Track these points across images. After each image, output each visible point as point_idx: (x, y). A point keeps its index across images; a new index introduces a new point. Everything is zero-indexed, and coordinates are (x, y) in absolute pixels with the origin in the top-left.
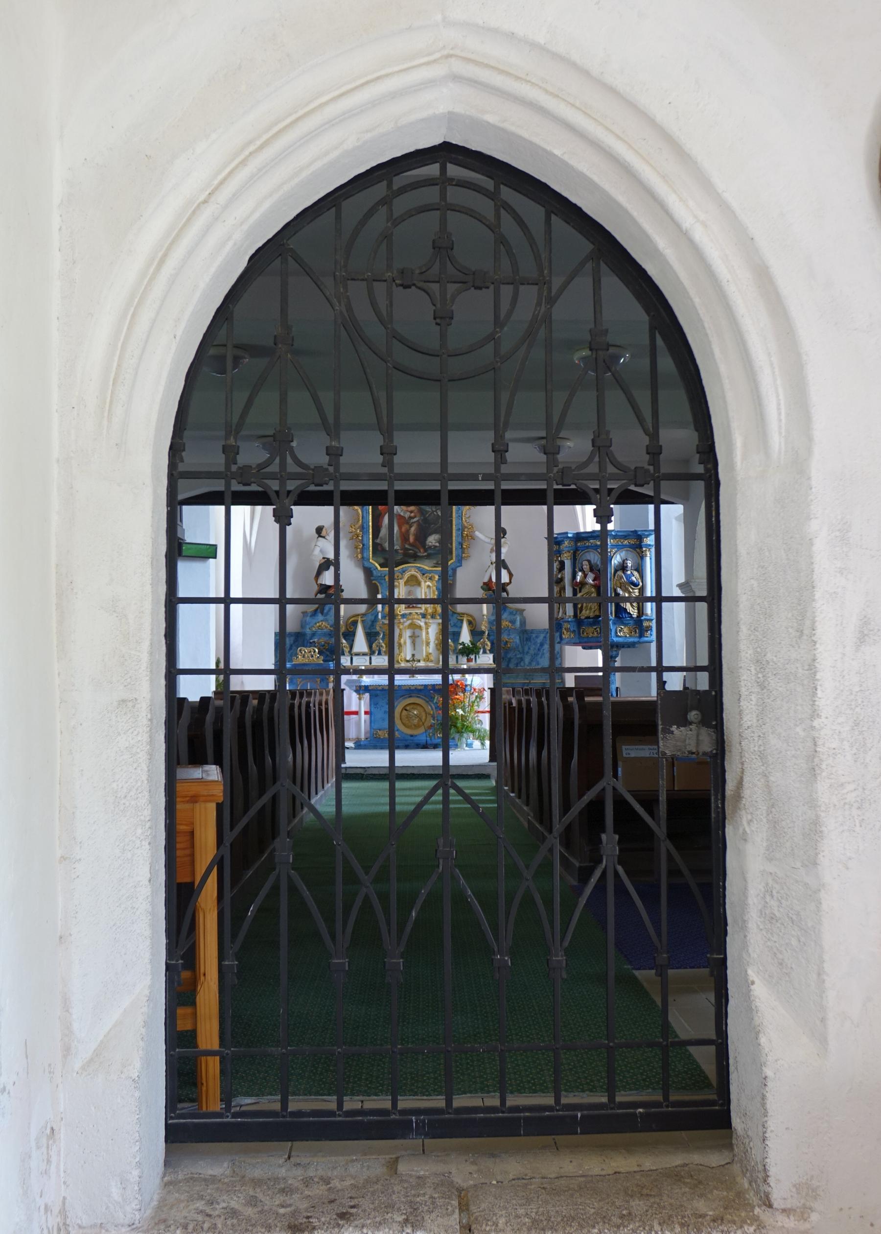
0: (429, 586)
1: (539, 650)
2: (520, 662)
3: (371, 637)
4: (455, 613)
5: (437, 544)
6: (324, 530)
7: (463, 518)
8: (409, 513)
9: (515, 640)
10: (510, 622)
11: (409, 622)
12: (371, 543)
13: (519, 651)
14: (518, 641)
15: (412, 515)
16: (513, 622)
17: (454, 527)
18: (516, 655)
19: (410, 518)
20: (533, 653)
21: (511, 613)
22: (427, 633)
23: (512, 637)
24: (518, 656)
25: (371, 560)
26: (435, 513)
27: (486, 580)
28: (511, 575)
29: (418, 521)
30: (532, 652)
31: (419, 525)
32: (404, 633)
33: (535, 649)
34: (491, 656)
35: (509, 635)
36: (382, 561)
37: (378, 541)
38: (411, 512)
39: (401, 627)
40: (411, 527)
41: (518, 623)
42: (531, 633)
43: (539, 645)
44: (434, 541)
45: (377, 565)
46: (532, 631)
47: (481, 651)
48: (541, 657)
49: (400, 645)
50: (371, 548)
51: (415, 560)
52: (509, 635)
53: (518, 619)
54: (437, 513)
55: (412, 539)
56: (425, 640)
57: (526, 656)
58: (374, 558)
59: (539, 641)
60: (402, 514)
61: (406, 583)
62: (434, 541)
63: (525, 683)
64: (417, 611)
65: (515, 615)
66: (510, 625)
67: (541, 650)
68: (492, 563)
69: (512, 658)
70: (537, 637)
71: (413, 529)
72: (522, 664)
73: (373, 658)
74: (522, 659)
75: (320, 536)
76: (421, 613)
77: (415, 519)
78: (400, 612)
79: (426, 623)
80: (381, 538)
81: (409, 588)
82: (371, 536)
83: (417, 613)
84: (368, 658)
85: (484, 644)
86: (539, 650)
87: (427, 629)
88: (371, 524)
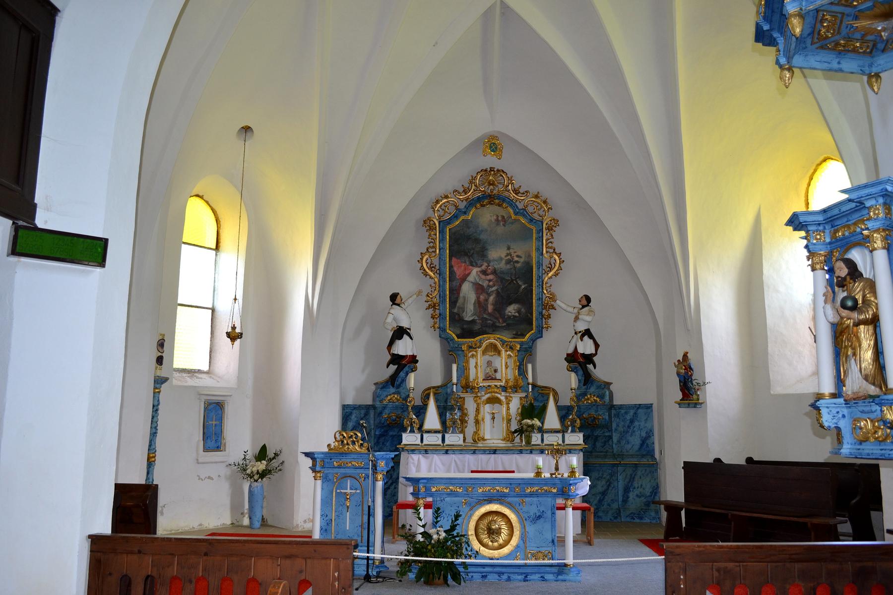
0: (510, 356)
1: (629, 427)
2: (608, 441)
3: (442, 412)
4: (536, 386)
5: (517, 314)
6: (398, 297)
7: (544, 286)
8: (487, 282)
9: (604, 417)
10: (597, 397)
11: (488, 396)
12: (448, 313)
13: (607, 428)
14: (607, 418)
15: (491, 283)
16: (602, 397)
17: (534, 296)
18: (604, 433)
19: (489, 286)
20: (622, 430)
21: (599, 387)
22: (508, 409)
23: (601, 413)
24: (607, 434)
25: (448, 331)
26: (514, 282)
27: (571, 351)
28: (597, 346)
29: (497, 290)
30: (621, 429)
31: (498, 293)
32: (482, 408)
33: (624, 426)
34: (581, 435)
35: (596, 411)
36: (458, 332)
37: (456, 311)
38: (490, 281)
39: (479, 401)
40: (489, 295)
41: (607, 398)
42: (620, 408)
43: (628, 422)
44: (513, 311)
45: (454, 335)
46: (621, 407)
47: (570, 428)
48: (631, 435)
49: (477, 422)
50: (448, 318)
51: (494, 331)
52: (596, 411)
53: (607, 393)
54: (516, 281)
55: (490, 308)
56: (505, 416)
57: (614, 434)
58: (451, 329)
59: (628, 417)
60: (480, 283)
61: (484, 353)
62: (513, 311)
63: (615, 464)
64: (496, 384)
65: (603, 389)
66: (598, 399)
67: (632, 428)
68: (576, 333)
69: (600, 436)
70: (626, 413)
71: (491, 298)
72: (610, 442)
73: (447, 436)
74: (610, 437)
75: (394, 304)
76: (501, 386)
77: (494, 289)
78: (477, 385)
79: (506, 398)
80: (459, 308)
81: (487, 358)
82: (448, 306)
83: (496, 386)
84: (440, 436)
85: (573, 422)
86: (629, 427)
87: (508, 404)
88: (448, 293)
